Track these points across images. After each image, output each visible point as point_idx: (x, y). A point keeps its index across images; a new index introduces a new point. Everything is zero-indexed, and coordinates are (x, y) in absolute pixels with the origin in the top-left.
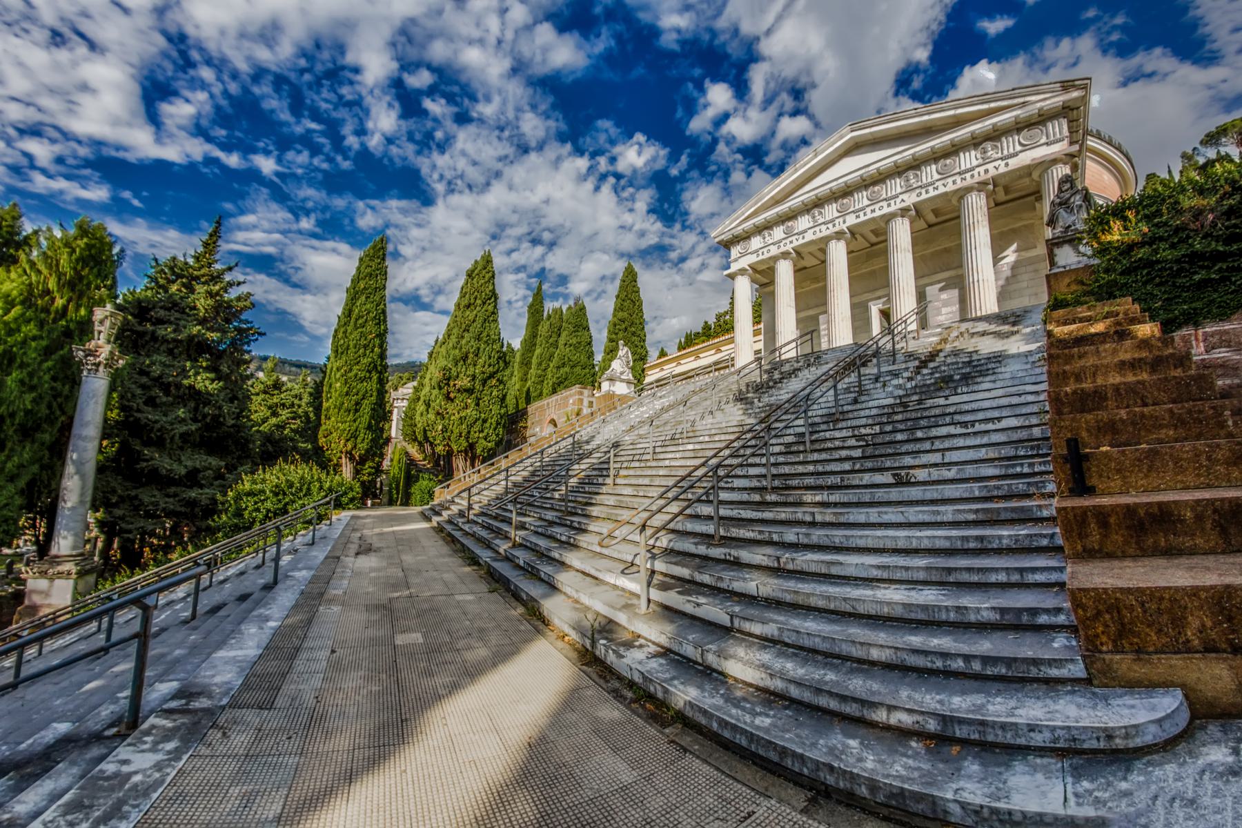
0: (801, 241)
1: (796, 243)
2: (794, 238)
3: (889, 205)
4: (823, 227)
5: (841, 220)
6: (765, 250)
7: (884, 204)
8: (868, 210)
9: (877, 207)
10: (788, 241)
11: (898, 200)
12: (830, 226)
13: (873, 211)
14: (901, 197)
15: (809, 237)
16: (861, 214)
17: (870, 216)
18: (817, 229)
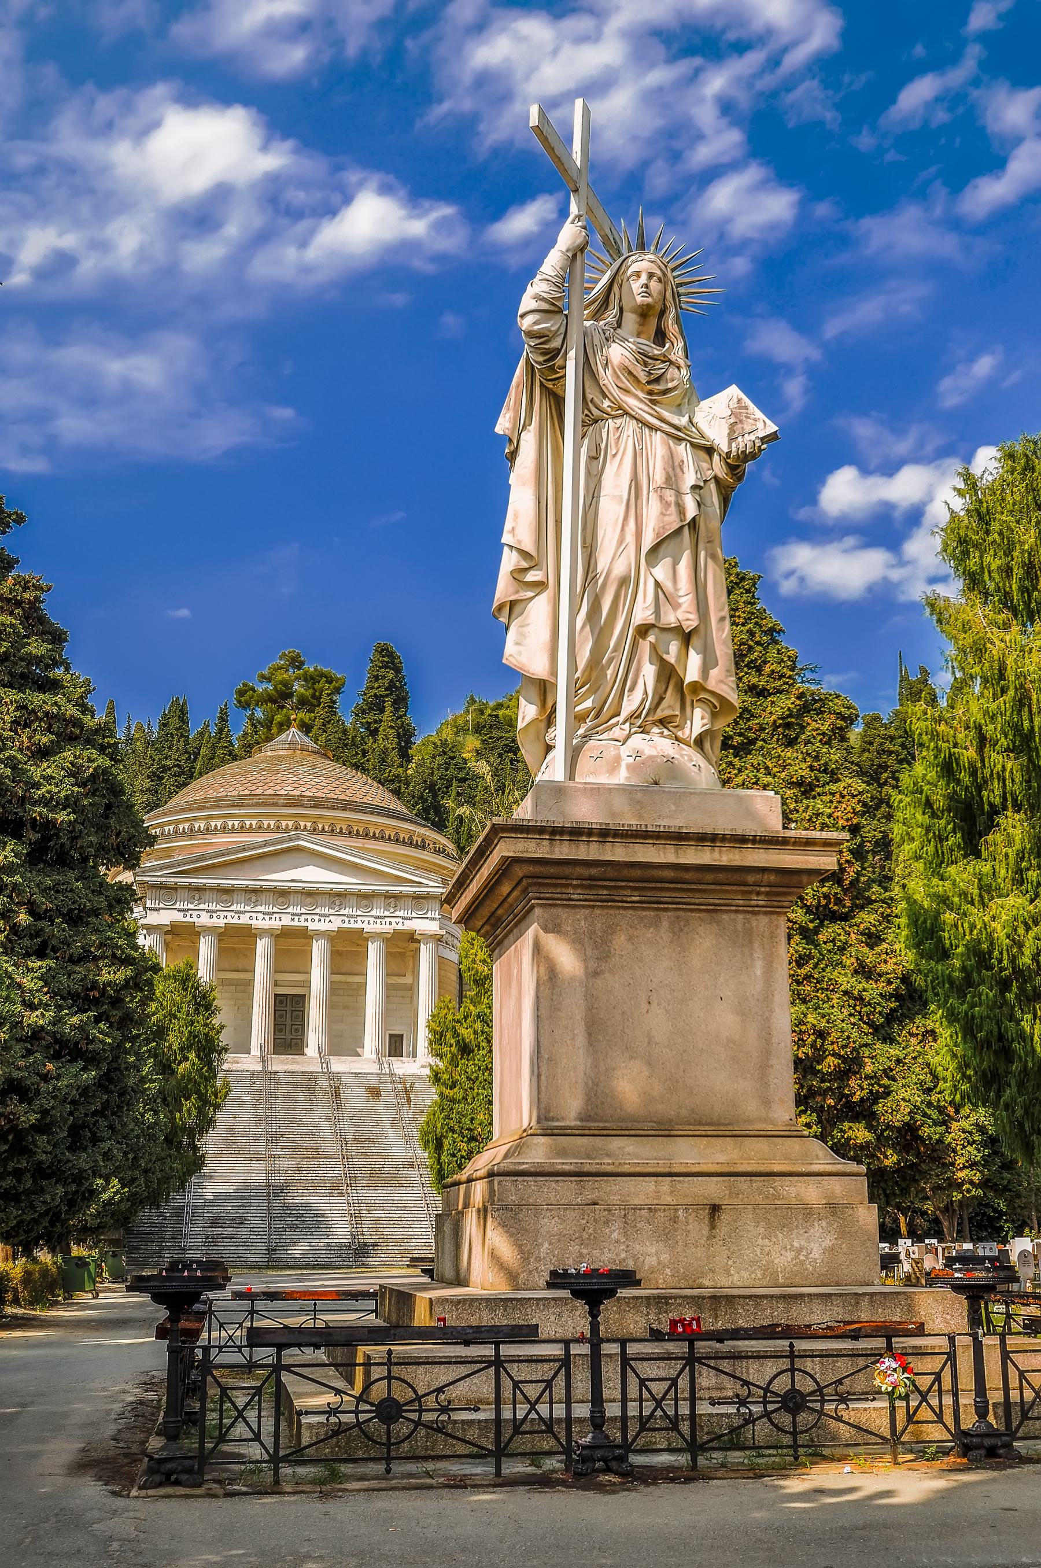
0: (235, 921)
1: (230, 921)
2: (229, 914)
3: (320, 920)
4: (261, 916)
5: (278, 916)
6: (195, 913)
7: (317, 918)
8: (303, 917)
9: (310, 917)
10: (222, 914)
11: (327, 919)
12: (267, 917)
13: (307, 920)
14: (331, 918)
15: (244, 919)
16: (296, 918)
17: (303, 924)
18: (254, 915)
